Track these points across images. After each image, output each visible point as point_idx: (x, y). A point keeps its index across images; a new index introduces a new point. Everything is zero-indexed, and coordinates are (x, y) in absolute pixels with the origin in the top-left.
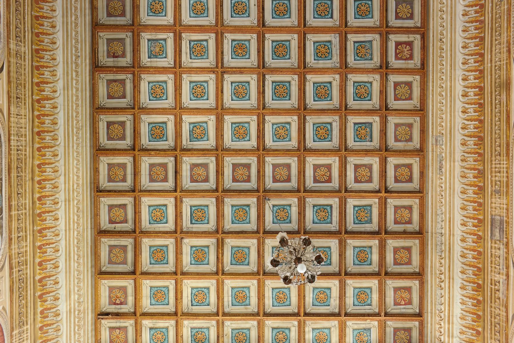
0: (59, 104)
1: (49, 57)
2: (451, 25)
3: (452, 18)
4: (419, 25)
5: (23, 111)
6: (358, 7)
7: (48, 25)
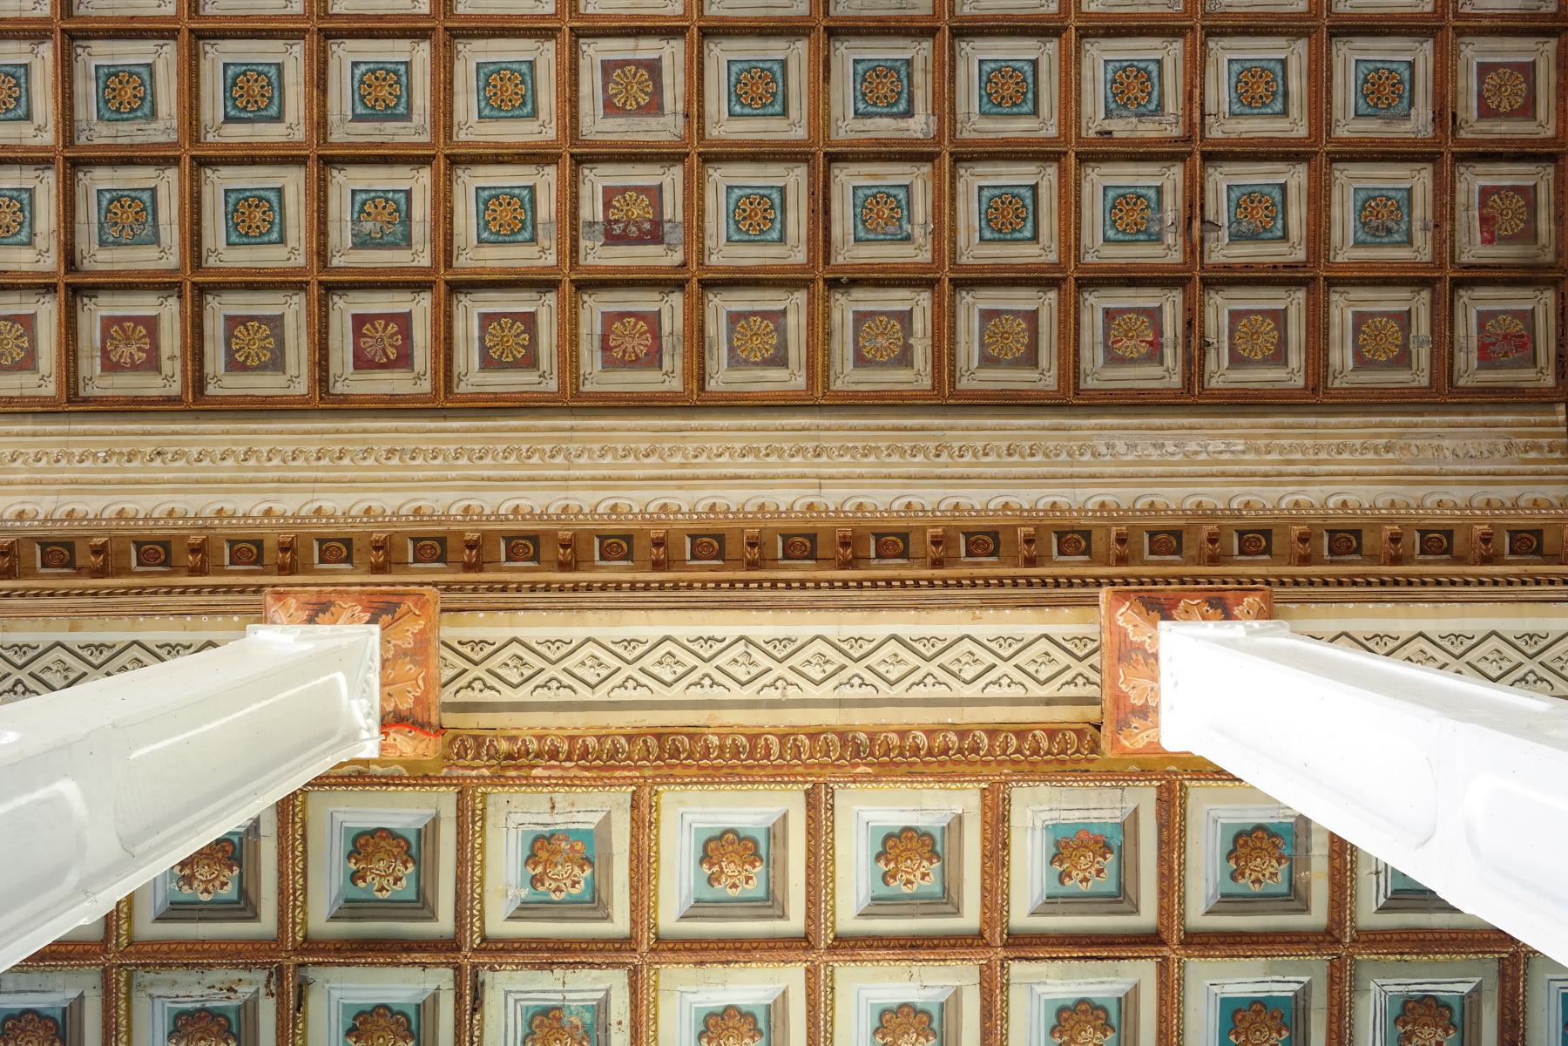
2: (197, 482)
3: (222, 482)
4: (211, 390)
6: (261, 199)
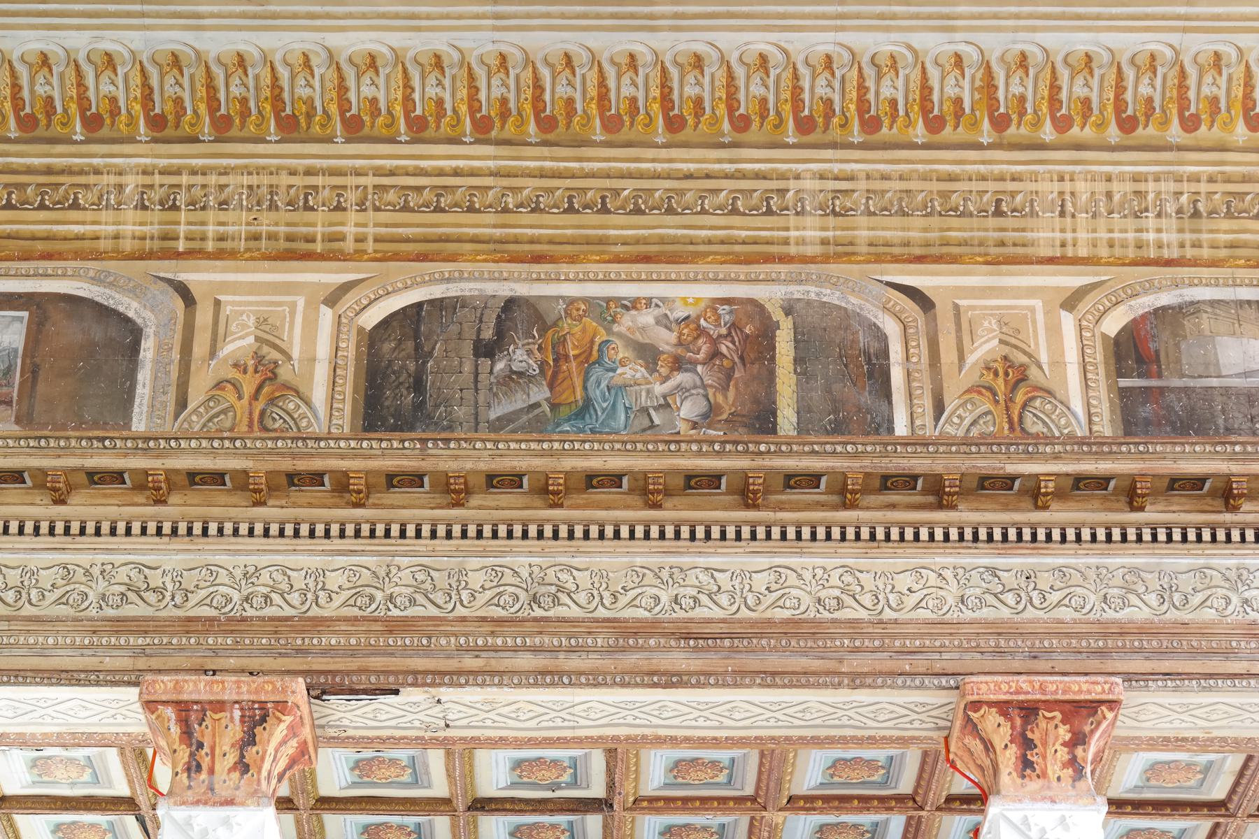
0: (1010, 46)
1: (821, 81)
5: (1043, 186)
7: (693, 81)
